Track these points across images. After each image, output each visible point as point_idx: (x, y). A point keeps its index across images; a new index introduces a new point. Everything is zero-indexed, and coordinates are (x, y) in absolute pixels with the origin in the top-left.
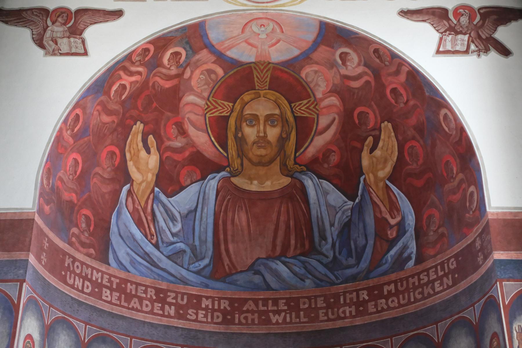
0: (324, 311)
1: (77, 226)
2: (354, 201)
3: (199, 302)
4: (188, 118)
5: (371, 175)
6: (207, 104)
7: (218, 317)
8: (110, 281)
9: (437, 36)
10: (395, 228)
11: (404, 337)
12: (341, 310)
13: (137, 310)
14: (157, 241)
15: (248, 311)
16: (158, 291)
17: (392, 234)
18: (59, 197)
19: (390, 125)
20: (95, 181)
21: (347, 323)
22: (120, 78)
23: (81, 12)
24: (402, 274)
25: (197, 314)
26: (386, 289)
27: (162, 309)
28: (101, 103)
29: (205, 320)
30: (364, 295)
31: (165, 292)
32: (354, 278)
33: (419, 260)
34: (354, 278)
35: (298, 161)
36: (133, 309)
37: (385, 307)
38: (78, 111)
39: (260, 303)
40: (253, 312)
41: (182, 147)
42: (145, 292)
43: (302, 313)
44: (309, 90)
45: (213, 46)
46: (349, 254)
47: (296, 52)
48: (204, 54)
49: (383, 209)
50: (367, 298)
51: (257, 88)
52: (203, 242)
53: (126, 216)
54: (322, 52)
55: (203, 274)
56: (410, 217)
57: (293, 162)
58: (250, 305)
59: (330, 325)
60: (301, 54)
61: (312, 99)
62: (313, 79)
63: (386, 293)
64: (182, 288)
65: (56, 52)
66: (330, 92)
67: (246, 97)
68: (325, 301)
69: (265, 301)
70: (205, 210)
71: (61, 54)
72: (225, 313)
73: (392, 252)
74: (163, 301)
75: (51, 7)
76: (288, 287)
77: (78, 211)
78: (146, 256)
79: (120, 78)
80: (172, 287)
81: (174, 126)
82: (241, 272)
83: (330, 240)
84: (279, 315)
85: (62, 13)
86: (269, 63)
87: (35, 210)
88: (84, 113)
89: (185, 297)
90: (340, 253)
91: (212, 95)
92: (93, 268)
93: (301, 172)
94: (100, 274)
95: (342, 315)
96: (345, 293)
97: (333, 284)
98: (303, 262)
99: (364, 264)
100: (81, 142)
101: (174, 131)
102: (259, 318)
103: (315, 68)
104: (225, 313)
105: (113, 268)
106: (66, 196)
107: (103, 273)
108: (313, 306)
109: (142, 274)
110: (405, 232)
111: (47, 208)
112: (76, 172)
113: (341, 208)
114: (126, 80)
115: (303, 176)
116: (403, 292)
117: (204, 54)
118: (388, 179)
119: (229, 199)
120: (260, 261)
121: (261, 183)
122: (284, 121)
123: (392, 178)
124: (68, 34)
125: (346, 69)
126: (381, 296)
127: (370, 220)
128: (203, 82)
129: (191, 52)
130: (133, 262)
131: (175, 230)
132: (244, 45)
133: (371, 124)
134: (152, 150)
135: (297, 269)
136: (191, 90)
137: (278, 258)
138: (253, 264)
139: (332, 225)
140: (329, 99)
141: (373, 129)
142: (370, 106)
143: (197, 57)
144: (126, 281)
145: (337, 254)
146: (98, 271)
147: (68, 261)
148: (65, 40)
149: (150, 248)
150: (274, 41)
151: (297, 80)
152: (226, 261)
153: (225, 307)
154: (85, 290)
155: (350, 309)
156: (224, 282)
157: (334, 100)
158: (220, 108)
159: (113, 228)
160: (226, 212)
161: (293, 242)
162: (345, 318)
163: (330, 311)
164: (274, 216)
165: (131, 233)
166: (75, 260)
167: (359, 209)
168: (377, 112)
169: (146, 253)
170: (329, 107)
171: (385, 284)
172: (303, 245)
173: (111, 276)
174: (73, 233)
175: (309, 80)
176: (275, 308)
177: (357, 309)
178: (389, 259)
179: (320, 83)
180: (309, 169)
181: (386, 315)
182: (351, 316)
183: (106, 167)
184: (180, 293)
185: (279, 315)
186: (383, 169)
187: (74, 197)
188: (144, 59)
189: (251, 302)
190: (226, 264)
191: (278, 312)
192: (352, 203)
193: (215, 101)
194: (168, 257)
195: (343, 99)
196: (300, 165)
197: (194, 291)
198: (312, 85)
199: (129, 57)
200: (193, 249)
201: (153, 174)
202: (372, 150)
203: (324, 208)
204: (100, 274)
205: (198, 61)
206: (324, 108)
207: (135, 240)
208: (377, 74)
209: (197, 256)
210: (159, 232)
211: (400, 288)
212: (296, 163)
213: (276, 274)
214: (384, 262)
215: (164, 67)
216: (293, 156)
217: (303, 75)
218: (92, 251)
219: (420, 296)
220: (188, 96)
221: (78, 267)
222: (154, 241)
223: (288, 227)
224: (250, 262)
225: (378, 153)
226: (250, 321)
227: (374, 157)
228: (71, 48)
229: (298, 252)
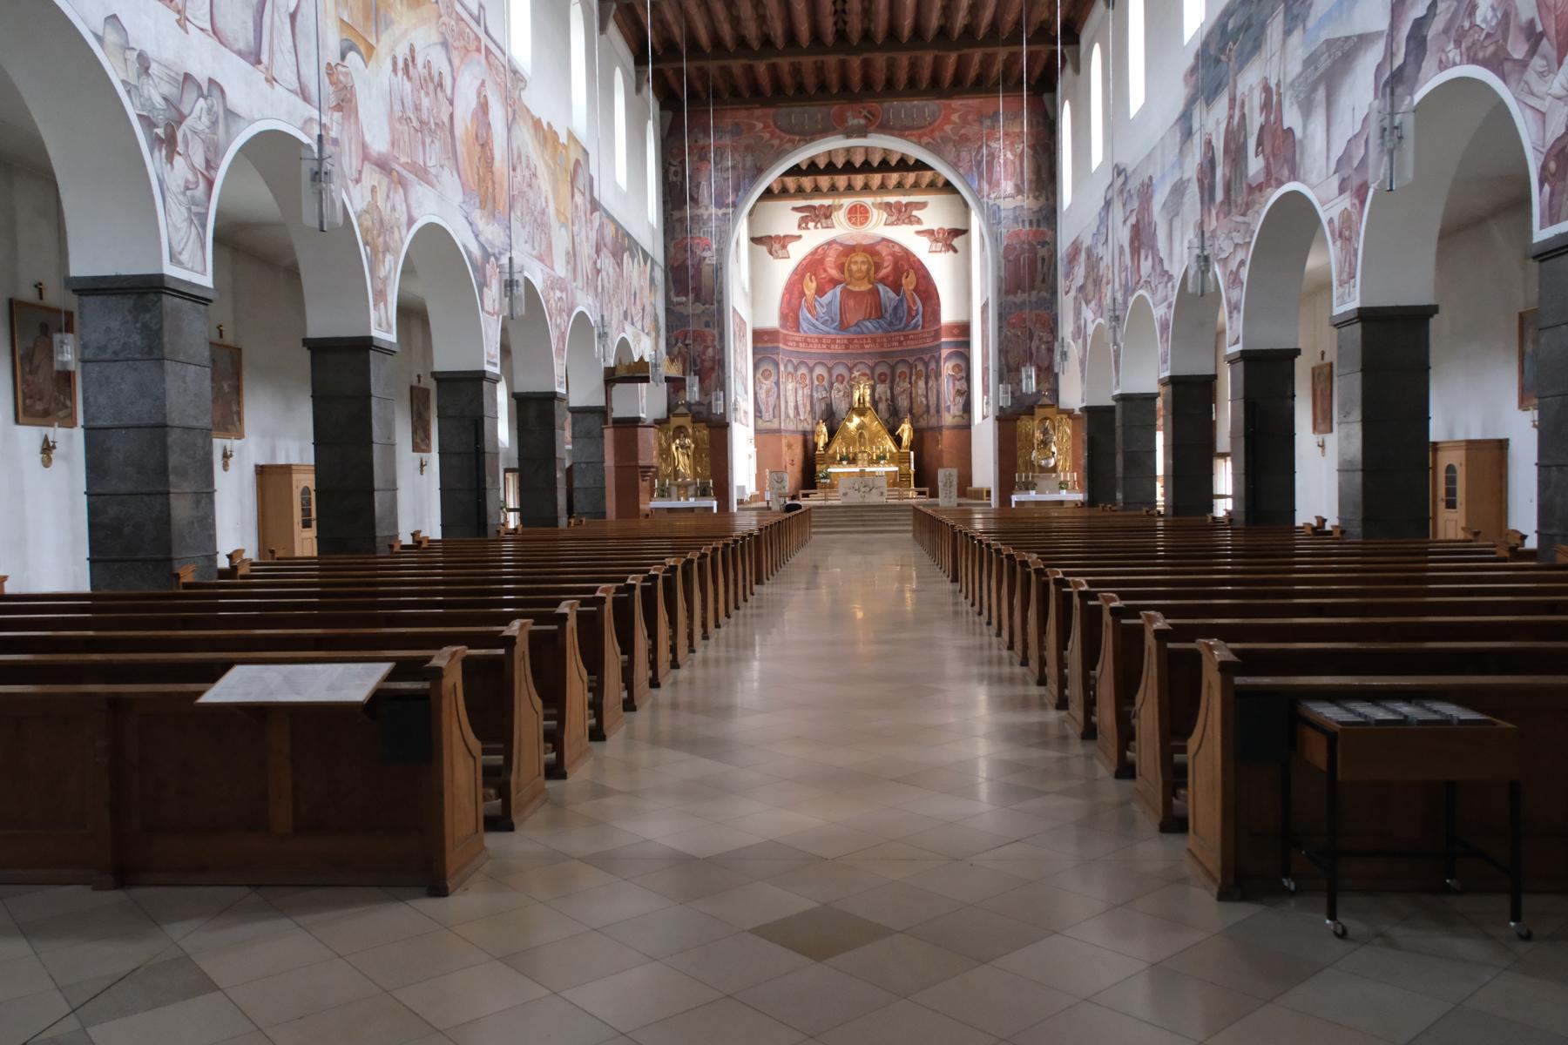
9: (929, 243)
17: (914, 313)
21: (895, 349)
23: (785, 237)
30: (902, 338)
32: (898, 330)
34: (898, 330)
75: (773, 235)
105: (802, 334)
181: (909, 348)
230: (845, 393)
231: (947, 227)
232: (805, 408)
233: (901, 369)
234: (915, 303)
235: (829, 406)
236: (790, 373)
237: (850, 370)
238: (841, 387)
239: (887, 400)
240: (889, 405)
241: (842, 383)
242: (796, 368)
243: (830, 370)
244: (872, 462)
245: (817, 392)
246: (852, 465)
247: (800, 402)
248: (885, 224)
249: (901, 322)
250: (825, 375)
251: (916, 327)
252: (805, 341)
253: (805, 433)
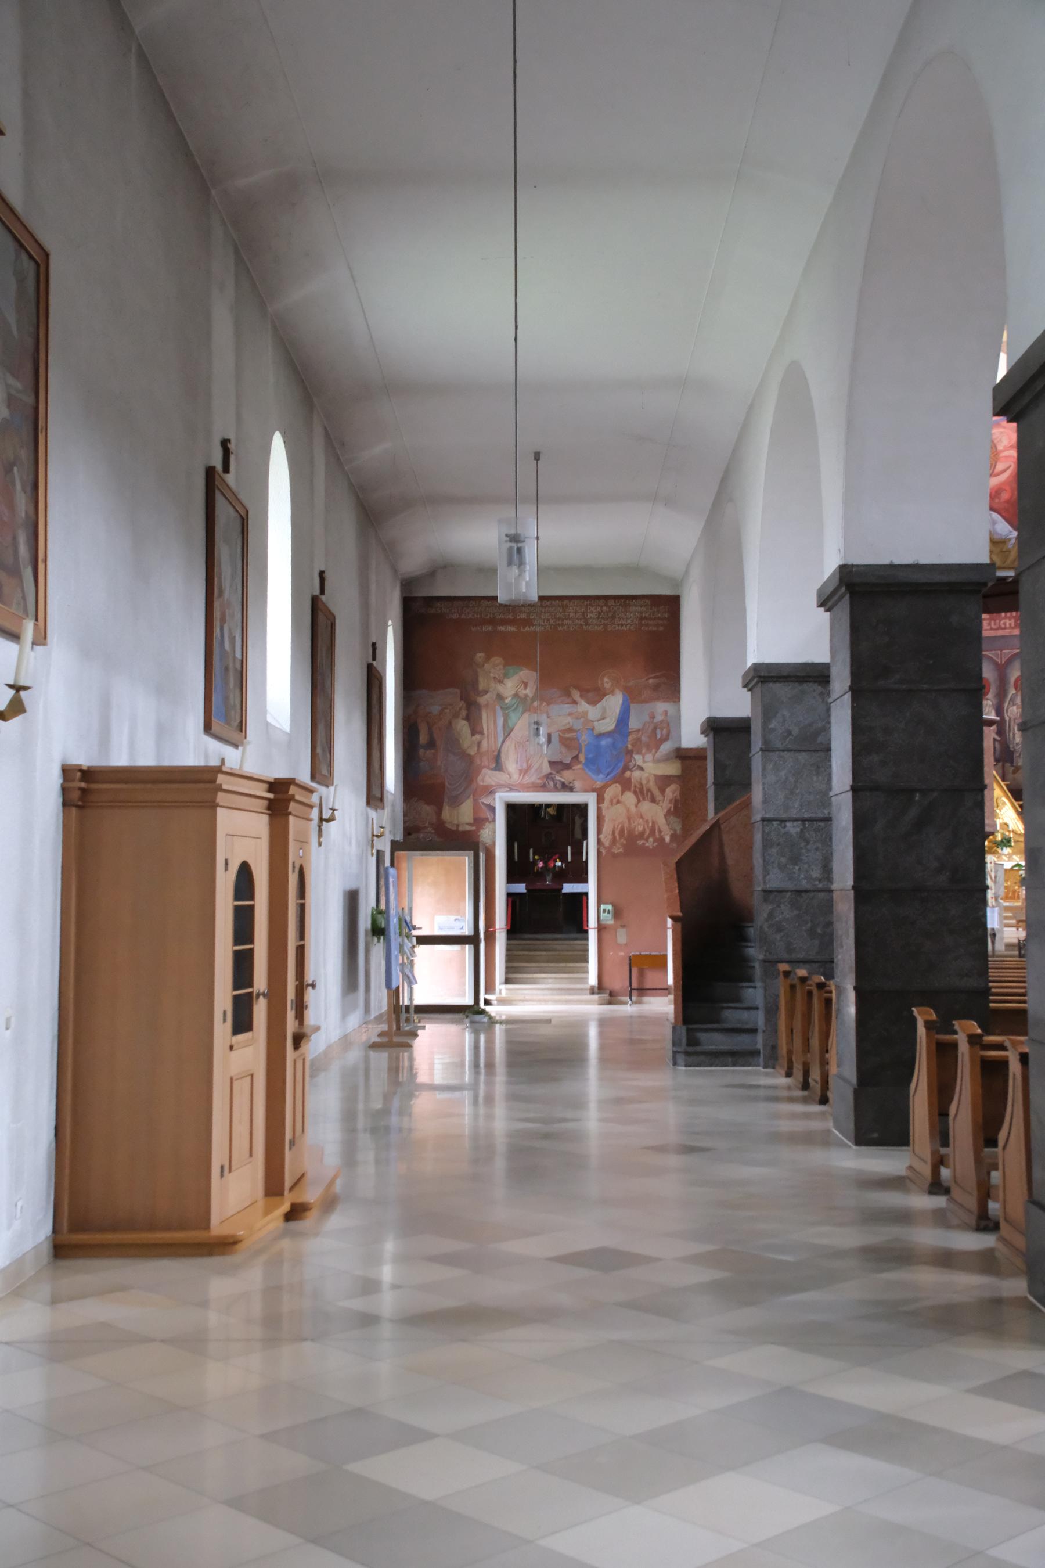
0: (988, 622)
12: (1002, 622)
21: (1006, 632)
95: (1003, 626)
155: (1010, 622)
162: (1005, 628)
170: (1006, 457)
182: (1011, 627)
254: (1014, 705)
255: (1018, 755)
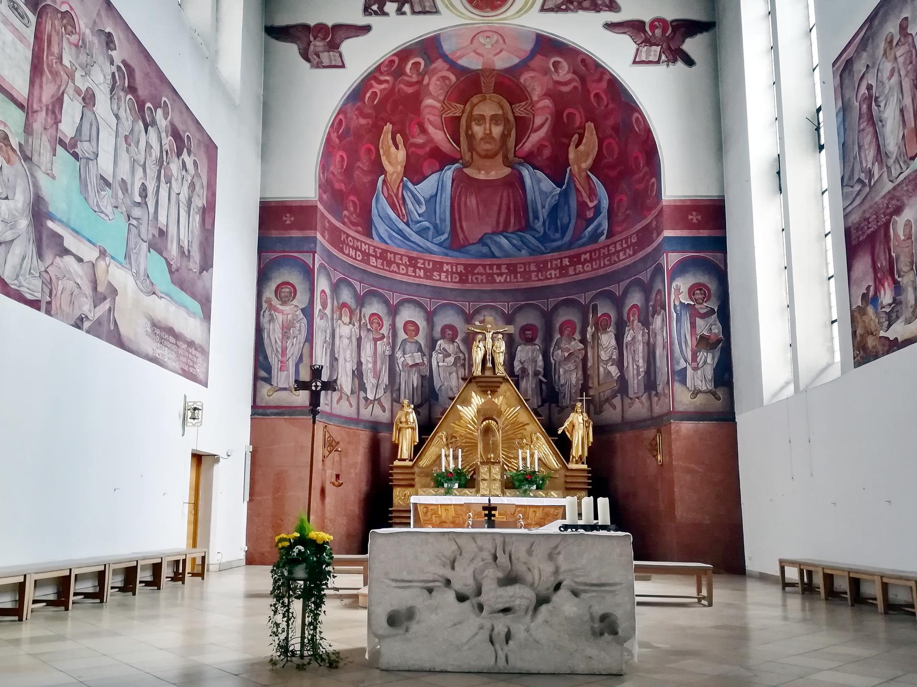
0: (536, 273)
1: (347, 209)
2: (561, 187)
3: (442, 267)
4: (428, 119)
5: (575, 166)
6: (443, 106)
7: (456, 278)
8: (374, 251)
9: (635, 46)
10: (593, 210)
11: (594, 292)
12: (548, 273)
13: (395, 272)
14: (408, 220)
15: (478, 274)
16: (411, 259)
17: (590, 214)
18: (333, 188)
19: (592, 125)
20: (357, 173)
22: (372, 86)
23: (337, 27)
24: (595, 246)
25: (440, 276)
26: (583, 257)
27: (414, 271)
28: (358, 109)
29: (446, 280)
30: (566, 262)
31: (416, 259)
33: (610, 234)
34: (558, 249)
35: (517, 154)
36: (393, 272)
37: (582, 270)
38: (341, 116)
39: (487, 267)
40: (482, 274)
41: (423, 143)
42: (401, 259)
43: (519, 275)
44: (527, 94)
45: (447, 56)
46: (556, 231)
47: (516, 61)
48: (439, 64)
49: (584, 194)
50: (568, 264)
51: (483, 91)
52: (443, 220)
53: (383, 201)
54: (538, 61)
55: (444, 245)
56: (605, 201)
57: (513, 155)
58: (480, 269)
59: (539, 284)
60: (520, 62)
61: (529, 101)
62: (530, 85)
63: (582, 260)
64: (428, 256)
65: (320, 65)
66: (544, 95)
67: (475, 100)
68: (537, 266)
69: (491, 266)
70: (444, 196)
71: (324, 67)
72: (460, 274)
73: (589, 229)
74: (415, 267)
76: (507, 255)
77: (347, 197)
78: (400, 232)
79: (372, 86)
80: (420, 255)
81: (416, 126)
82: (473, 244)
83: (541, 219)
84: (502, 276)
85: (322, 28)
86: (494, 70)
87: (317, 199)
88: (346, 118)
89: (431, 263)
90: (549, 230)
91: (446, 98)
92: (362, 242)
93: (520, 164)
94: (367, 246)
95: (549, 277)
96: (551, 261)
97: (543, 253)
98: (520, 237)
99: (567, 238)
100: (344, 142)
101: (416, 129)
102: (487, 278)
103: (532, 74)
104: (460, 274)
105: (376, 241)
106: (338, 186)
107: (369, 245)
108: (527, 270)
109: (399, 246)
110: (600, 213)
111: (325, 196)
112: (343, 167)
113: (552, 192)
114: (377, 88)
115: (521, 167)
116: (595, 260)
117: (439, 64)
118: (589, 170)
119: (462, 186)
120: (487, 236)
121: (487, 173)
122: (507, 120)
123: (592, 169)
124: (327, 48)
125: (558, 75)
126: (579, 262)
127: (573, 204)
128: (440, 87)
129: (428, 61)
130: (390, 236)
131: (420, 212)
132: (473, 54)
133: (577, 123)
134: (400, 146)
135: (515, 242)
136: (430, 95)
137: (501, 233)
138: (482, 237)
139: (543, 207)
140: (542, 102)
141: (579, 128)
142: (577, 109)
143: (434, 66)
144: (385, 251)
145: (547, 231)
146: (366, 244)
147: (343, 237)
148: (326, 54)
149: (402, 226)
150: (498, 50)
151: (518, 85)
152: (461, 236)
153: (461, 271)
154: (357, 258)
156: (460, 252)
157: (547, 102)
158: (453, 109)
159: (374, 211)
160: (460, 197)
161: (512, 220)
162: (551, 278)
163: (540, 274)
164: (498, 199)
165: (387, 214)
166: (348, 236)
167: (565, 195)
168: (582, 113)
169: (400, 230)
171: (582, 253)
172: (520, 223)
173: (375, 247)
174: (345, 215)
175: (527, 84)
176: (498, 271)
177: (560, 272)
178: (587, 234)
179: (536, 87)
180: (526, 162)
183: (365, 161)
184: (427, 260)
185: (502, 276)
186: (585, 161)
187: (343, 187)
188: (390, 69)
189: (480, 267)
190: (461, 239)
191: (501, 274)
192: (560, 189)
193: (449, 104)
194: (417, 233)
195: (555, 102)
196: (519, 158)
197: (437, 258)
198: (529, 89)
199: (378, 69)
200: (435, 226)
201: (402, 167)
202: (577, 146)
203: (537, 193)
204: (367, 246)
205: (435, 69)
206: (538, 109)
207: (391, 220)
208: (583, 80)
209: (439, 232)
210: (409, 213)
211: (593, 257)
212: (515, 156)
213: (500, 247)
214: (583, 235)
215: (407, 76)
216: (513, 151)
217: (522, 81)
218: (360, 229)
219: (609, 263)
220: (427, 99)
221: (350, 241)
222: (405, 221)
223: (509, 208)
224: (479, 236)
225: (581, 148)
226: (479, 281)
227: (579, 151)
228: (331, 61)
229: (517, 228)
230: (457, 359)
231: (670, 16)
232: (377, 376)
233: (564, 316)
234: (592, 193)
235: (427, 381)
236: (344, 305)
237: (469, 319)
238: (450, 348)
239: (536, 373)
240: (541, 382)
241: (452, 340)
242: (361, 301)
243: (430, 317)
244: (512, 484)
245: (404, 353)
246: (466, 491)
247: (367, 366)
248: (543, 9)
249: (563, 234)
250: (422, 324)
251: (595, 236)
252: (383, 256)
253: (375, 428)
254: (559, 349)
255: (562, 395)
